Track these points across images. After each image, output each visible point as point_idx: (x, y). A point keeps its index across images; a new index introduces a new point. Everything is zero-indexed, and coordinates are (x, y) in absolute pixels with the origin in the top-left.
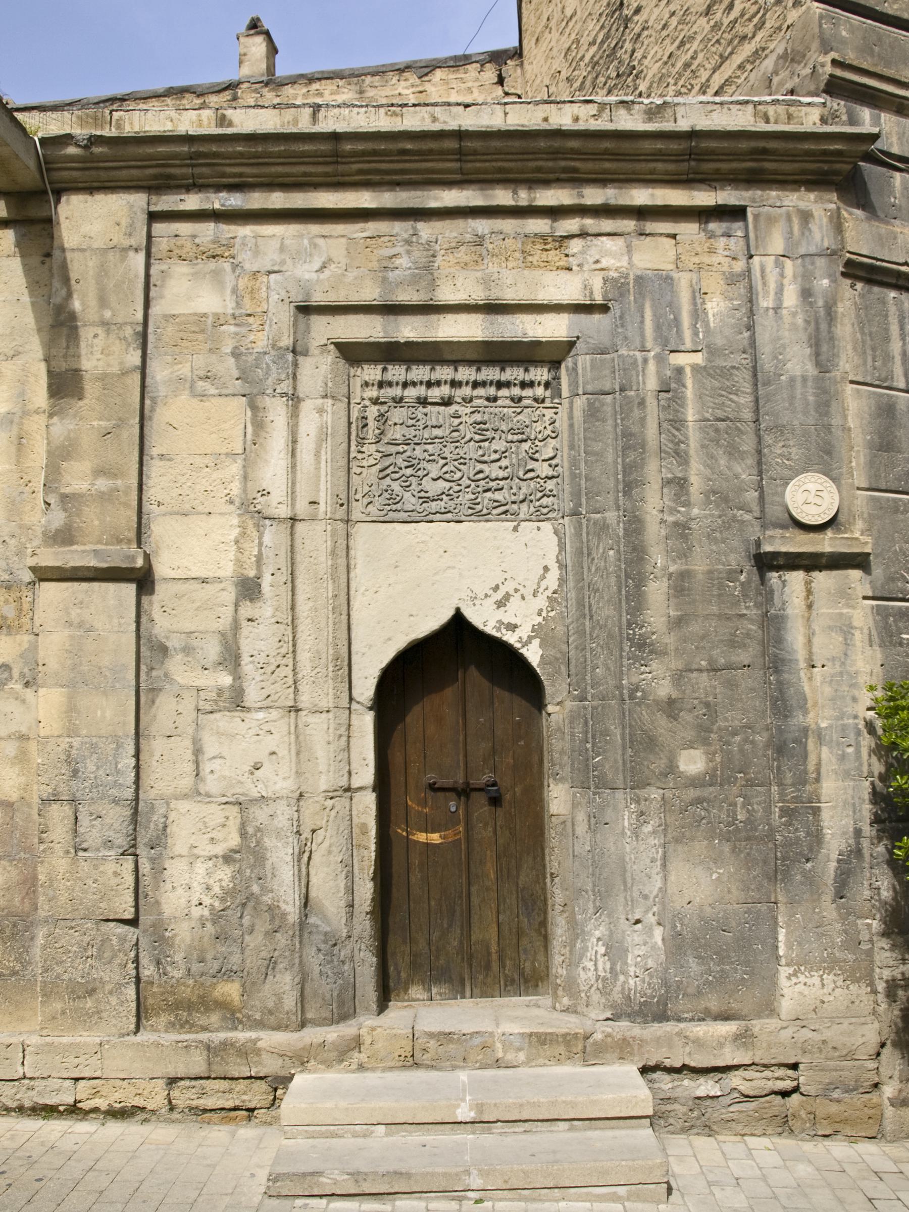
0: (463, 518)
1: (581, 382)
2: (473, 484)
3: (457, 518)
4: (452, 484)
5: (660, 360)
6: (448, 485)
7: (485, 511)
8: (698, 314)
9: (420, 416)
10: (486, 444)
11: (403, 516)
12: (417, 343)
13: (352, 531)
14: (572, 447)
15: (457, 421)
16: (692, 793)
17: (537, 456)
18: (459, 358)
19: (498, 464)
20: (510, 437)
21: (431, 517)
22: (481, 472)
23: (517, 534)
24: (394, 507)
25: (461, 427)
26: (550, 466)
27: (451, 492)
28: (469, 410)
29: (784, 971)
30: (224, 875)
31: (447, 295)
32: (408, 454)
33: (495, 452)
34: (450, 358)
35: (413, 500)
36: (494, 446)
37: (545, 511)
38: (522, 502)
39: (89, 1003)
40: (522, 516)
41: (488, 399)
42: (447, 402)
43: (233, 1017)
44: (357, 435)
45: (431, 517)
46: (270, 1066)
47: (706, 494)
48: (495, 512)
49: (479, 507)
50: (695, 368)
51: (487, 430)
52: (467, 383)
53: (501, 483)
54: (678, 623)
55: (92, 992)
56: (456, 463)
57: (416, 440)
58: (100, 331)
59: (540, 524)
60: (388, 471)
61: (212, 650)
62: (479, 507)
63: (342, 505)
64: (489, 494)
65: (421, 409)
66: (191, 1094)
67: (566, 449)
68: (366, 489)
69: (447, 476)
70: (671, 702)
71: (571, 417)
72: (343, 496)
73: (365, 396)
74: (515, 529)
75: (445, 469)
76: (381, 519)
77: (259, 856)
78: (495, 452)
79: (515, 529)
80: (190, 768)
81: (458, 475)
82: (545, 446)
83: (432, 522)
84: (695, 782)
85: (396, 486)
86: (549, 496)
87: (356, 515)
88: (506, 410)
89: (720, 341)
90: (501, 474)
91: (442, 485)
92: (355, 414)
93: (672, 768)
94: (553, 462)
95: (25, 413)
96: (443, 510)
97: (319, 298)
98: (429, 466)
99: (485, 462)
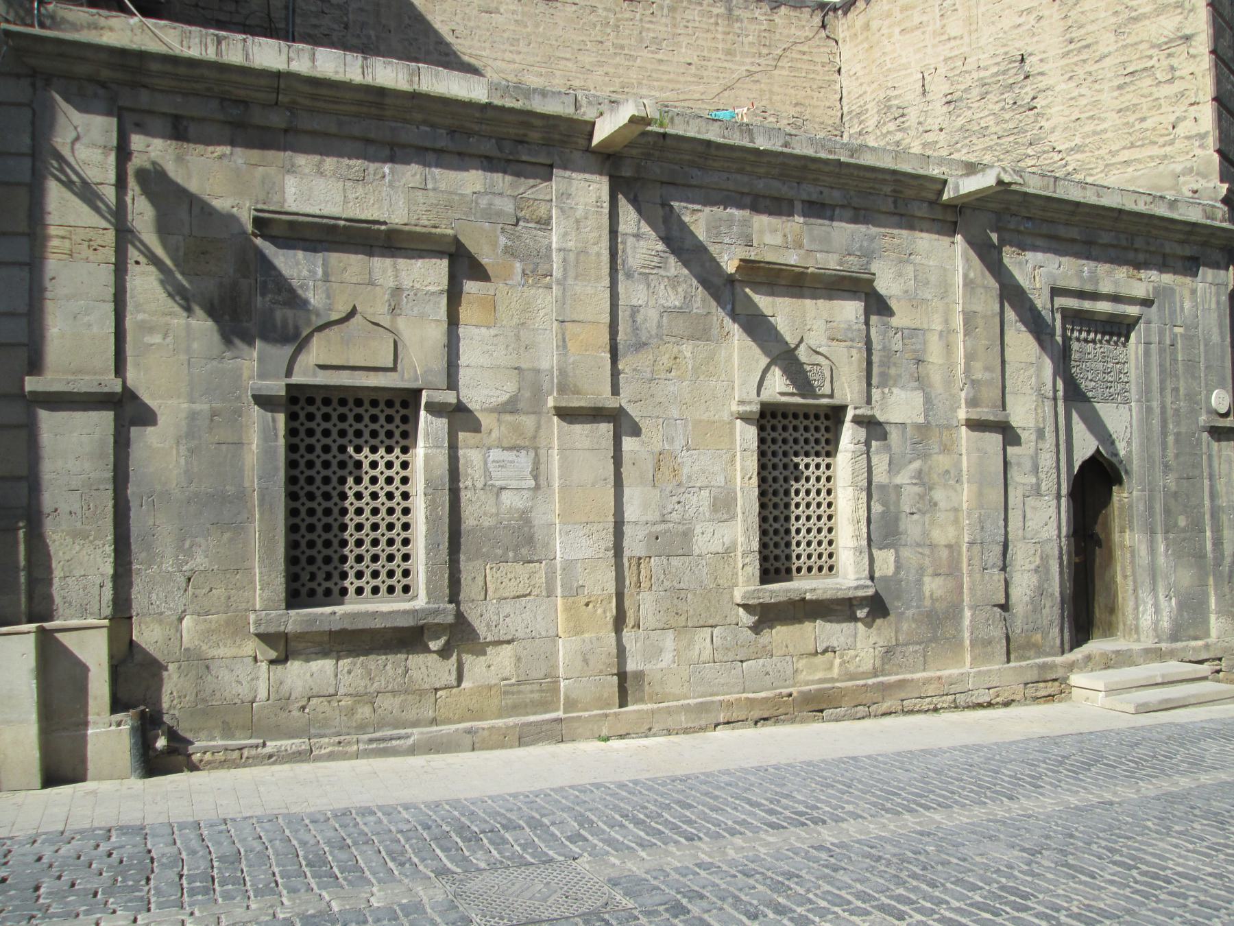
5: (1171, 330)
8: (1182, 308)
16: (1182, 535)
29: (1213, 617)
30: (1034, 579)
39: (989, 649)
43: (1039, 650)
46: (1060, 673)
47: (1186, 395)
50: (1182, 335)
54: (1177, 456)
55: (990, 643)
58: (982, 291)
61: (1028, 465)
66: (1033, 690)
70: (1176, 492)
71: (1137, 353)
77: (1047, 571)
80: (1021, 524)
84: (1184, 530)
89: (1189, 322)
93: (1176, 524)
95: (949, 332)
97: (1061, 284)
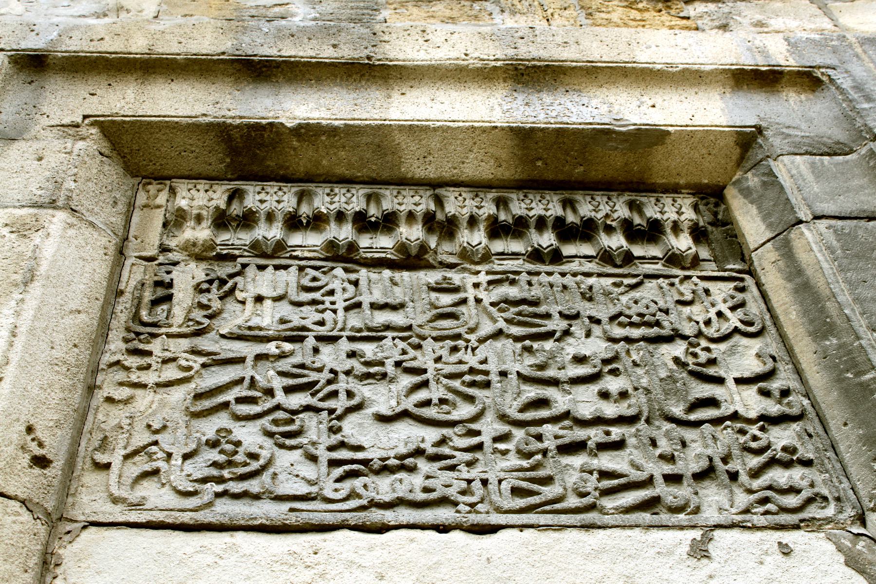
0: (496, 519)
1: (795, 199)
2: (519, 434)
3: (474, 519)
4: (447, 431)
6: (432, 435)
7: (573, 501)
9: (336, 285)
10: (549, 345)
11: (276, 511)
12: (332, 131)
13: (67, 552)
14: (822, 327)
15: (446, 299)
17: (711, 371)
18: (447, 172)
19: (594, 388)
20: (618, 332)
21: (377, 516)
22: (542, 403)
23: (706, 567)
24: (236, 487)
25: (463, 309)
26: (765, 393)
27: (445, 450)
28: (483, 278)
31: (403, 50)
32: (297, 359)
33: (580, 360)
34: (419, 171)
35: (309, 471)
36: (572, 347)
37: (792, 501)
38: (699, 477)
40: (710, 515)
41: (536, 255)
42: (411, 259)
44: (136, 317)
45: (377, 516)
48: (609, 503)
49: (549, 492)
51: (548, 316)
52: (473, 221)
53: (616, 432)
56: (456, 384)
57: (322, 331)
59: (787, 537)
60: (230, 396)
62: (549, 492)
63: (41, 462)
64: (578, 460)
65: (339, 272)
67: (806, 351)
68: (141, 438)
69: (431, 412)
72: (55, 446)
73: (172, 243)
74: (699, 552)
75: (422, 395)
76: (186, 518)
78: (580, 360)
79: (699, 552)
81: (464, 411)
82: (732, 351)
83: (382, 529)
85: (250, 436)
86: (787, 465)
87: (92, 500)
88: (591, 281)
90: (610, 410)
91: (405, 436)
92: (134, 275)
94: (775, 385)
96: (421, 496)
98: (365, 391)
99: (554, 382)
